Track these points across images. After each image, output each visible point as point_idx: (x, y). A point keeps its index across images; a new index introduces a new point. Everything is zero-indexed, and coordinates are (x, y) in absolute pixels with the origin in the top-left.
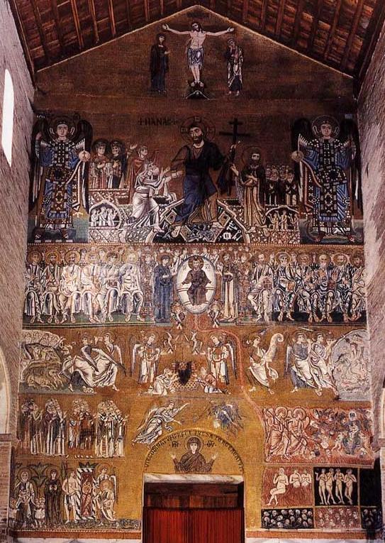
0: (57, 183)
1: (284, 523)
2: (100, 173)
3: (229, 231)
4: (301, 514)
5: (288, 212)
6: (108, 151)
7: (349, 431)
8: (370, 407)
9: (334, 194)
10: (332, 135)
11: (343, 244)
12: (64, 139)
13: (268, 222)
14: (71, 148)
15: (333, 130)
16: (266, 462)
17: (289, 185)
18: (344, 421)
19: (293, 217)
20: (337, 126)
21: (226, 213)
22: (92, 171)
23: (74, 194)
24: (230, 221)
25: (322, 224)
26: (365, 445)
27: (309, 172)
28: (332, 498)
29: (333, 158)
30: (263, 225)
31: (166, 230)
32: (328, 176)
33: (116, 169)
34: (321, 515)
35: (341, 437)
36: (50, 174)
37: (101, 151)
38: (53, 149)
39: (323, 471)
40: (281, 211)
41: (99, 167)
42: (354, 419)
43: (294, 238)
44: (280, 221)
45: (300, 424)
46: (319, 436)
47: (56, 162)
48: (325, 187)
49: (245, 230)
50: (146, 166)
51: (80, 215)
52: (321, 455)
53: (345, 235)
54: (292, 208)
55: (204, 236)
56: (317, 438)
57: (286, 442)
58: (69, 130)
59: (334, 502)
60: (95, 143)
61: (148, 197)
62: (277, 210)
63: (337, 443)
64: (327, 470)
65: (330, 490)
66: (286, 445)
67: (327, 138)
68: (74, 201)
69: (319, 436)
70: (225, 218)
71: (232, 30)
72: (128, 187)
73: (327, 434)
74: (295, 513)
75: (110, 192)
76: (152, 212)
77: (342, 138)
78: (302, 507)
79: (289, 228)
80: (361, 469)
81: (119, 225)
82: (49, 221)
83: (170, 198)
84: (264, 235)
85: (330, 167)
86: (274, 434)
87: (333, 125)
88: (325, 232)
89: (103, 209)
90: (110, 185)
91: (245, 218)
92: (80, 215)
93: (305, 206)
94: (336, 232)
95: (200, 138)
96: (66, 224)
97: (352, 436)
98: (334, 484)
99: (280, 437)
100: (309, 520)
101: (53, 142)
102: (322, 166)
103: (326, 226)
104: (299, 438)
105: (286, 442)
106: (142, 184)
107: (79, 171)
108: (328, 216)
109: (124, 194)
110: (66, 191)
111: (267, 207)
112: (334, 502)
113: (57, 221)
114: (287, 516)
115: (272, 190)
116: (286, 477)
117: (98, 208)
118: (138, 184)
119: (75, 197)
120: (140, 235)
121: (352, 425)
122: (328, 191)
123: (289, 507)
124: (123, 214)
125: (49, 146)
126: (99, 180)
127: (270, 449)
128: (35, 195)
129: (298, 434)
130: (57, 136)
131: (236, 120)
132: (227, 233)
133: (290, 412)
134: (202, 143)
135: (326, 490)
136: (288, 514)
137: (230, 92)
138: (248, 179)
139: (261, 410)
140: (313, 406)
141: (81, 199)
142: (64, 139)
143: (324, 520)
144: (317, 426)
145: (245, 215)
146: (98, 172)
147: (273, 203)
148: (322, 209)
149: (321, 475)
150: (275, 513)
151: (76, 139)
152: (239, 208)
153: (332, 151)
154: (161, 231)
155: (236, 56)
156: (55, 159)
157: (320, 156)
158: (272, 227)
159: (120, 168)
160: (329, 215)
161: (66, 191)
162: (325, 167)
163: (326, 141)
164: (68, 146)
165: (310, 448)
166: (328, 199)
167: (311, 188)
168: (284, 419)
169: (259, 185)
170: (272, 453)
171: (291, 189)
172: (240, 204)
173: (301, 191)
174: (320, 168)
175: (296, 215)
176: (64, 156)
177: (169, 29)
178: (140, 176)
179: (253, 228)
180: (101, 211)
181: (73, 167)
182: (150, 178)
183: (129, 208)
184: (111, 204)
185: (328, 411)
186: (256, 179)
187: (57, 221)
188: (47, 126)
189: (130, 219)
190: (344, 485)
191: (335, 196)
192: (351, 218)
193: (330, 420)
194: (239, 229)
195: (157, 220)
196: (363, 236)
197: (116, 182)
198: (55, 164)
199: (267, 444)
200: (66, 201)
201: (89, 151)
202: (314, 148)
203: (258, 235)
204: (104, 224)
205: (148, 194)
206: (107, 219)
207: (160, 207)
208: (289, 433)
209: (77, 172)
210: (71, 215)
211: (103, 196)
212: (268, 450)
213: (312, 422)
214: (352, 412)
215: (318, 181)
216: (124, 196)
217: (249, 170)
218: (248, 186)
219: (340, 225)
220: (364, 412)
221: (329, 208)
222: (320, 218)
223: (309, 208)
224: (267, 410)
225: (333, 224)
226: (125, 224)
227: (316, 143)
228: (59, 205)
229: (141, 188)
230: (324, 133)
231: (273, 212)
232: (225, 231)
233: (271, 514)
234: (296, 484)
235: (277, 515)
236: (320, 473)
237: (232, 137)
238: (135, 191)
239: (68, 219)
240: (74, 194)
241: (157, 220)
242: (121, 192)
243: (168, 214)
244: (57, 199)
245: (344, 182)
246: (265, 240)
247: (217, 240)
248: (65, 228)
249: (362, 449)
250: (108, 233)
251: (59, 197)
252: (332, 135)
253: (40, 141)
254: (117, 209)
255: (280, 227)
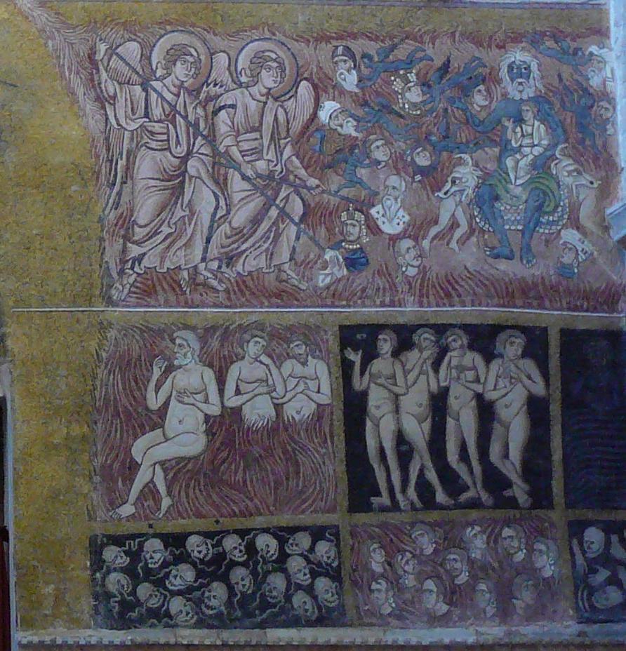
1: (199, 602)
4: (283, 557)
7: (506, 148)
8: (600, 33)
16: (110, 302)
18: (479, 100)
26: (584, 213)
28: (432, 476)
34: (377, 560)
35: (467, 174)
39: (386, 344)
42: (529, 92)
45: (269, 119)
46: (363, 173)
52: (374, 265)
56: (356, 182)
57: (205, 200)
59: (441, 497)
63: (449, 208)
64: (405, 338)
65: (418, 432)
66: (206, 219)
69: (363, 173)
73: (399, 164)
74: (251, 549)
78: (285, 519)
80: (564, 332)
86: (146, 166)
97: (519, 169)
98: (439, 404)
99: (175, 181)
100: (322, 584)
104: (268, 185)
105: (205, 200)
112: (441, 497)
114: (216, 568)
116: (209, 375)
121: (520, 120)
123: (227, 523)
127: (127, 238)
129: (261, 165)
133: (222, 59)
135: (400, 438)
136: (220, 558)
139: (83, 50)
140: (332, 27)
143: (395, 583)
144: (349, 128)
149: (377, 365)
150: (155, 552)
165: (322, 232)
168: (194, 92)
170: (139, 259)
185: (402, 53)
190: (486, 411)
193: (415, 95)
199: (112, 216)
208: (220, 167)
212: (118, 245)
213: (329, 107)
214: (518, 55)
220: (578, 59)
224: (112, 51)
233: (135, 556)
234: (258, 411)
235: (165, 564)
236: (370, 355)
249: (570, 235)
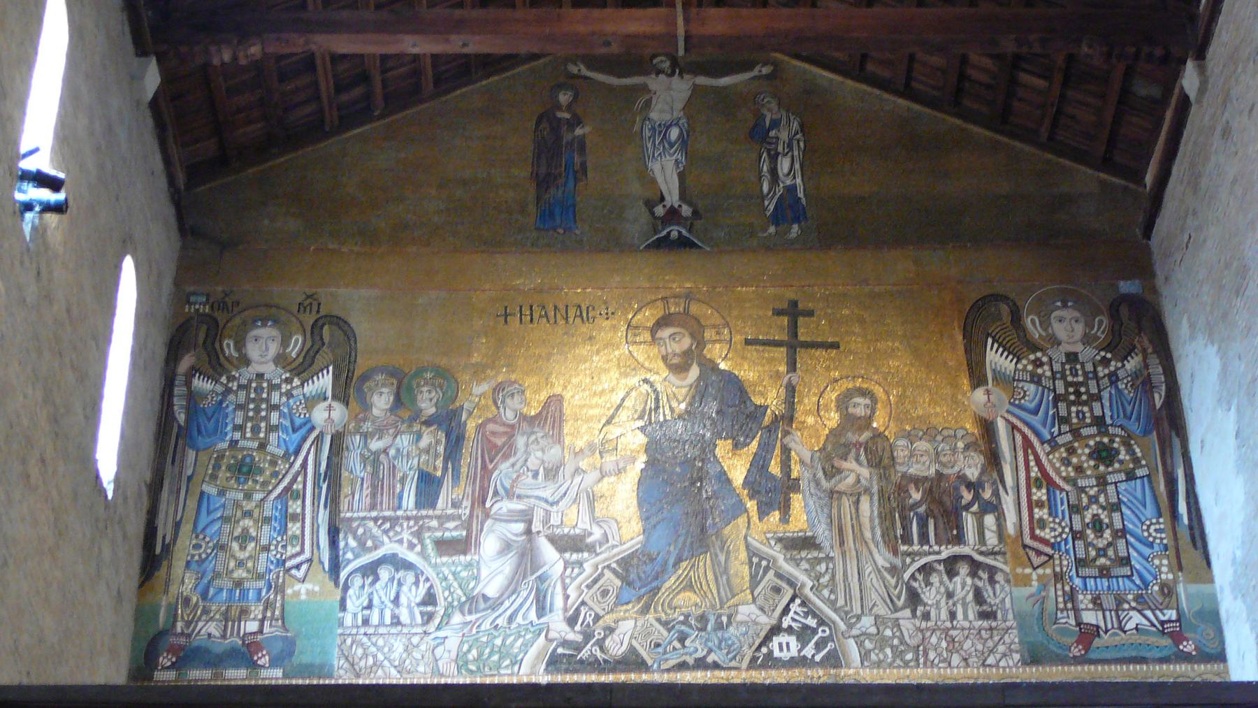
0: (240, 496)
2: (376, 463)
3: (790, 630)
5: (975, 567)
6: (401, 400)
9: (1115, 507)
10: (1087, 340)
11: (1162, 660)
12: (269, 369)
13: (914, 598)
14: (289, 395)
15: (1089, 325)
17: (969, 485)
19: (992, 581)
20: (1099, 312)
21: (779, 576)
22: (354, 464)
23: (294, 528)
24: (792, 600)
25: (1084, 600)
27: (1027, 444)
29: (1097, 406)
30: (896, 610)
31: (588, 636)
32: (1090, 456)
33: (427, 451)
36: (217, 467)
37: (381, 401)
38: (231, 397)
40: (951, 565)
41: (375, 445)
43: (1001, 648)
44: (950, 595)
47: (237, 435)
48: (1082, 490)
49: (842, 626)
50: (521, 441)
51: (308, 592)
53: (1163, 632)
54: (981, 553)
55: (710, 651)
58: (285, 343)
60: (365, 378)
61: (528, 532)
62: (939, 562)
67: (1071, 349)
68: (291, 550)
70: (777, 590)
71: (766, 70)
72: (467, 503)
75: (408, 518)
76: (541, 579)
77: (1117, 345)
79: (984, 615)
81: (437, 621)
82: (206, 611)
83: (597, 534)
84: (902, 641)
85: (1093, 430)
87: (1089, 312)
88: (1098, 627)
89: (384, 573)
90: (409, 500)
91: (841, 587)
92: (308, 592)
93: (1025, 546)
94: (1130, 626)
95: (687, 354)
96: (262, 621)
101: (234, 378)
102: (1065, 428)
103: (1097, 603)
106: (510, 494)
107: (313, 459)
108: (1102, 576)
109: (451, 525)
110: (267, 520)
111: (909, 554)
113: (234, 612)
115: (917, 504)
117: (371, 571)
118: (496, 493)
119: (295, 537)
120: (503, 652)
122: (1093, 500)
124: (449, 588)
125: (219, 389)
126: (374, 487)
128: (164, 529)
130: (245, 361)
131: (794, 304)
132: (783, 638)
134: (694, 372)
137: (772, 229)
138: (839, 471)
141: (316, 544)
142: (269, 369)
145: (839, 576)
146: (373, 461)
147: (924, 538)
148: (1081, 554)
151: (304, 368)
152: (818, 561)
153: (1092, 384)
154: (571, 636)
155: (784, 136)
156: (237, 428)
157: (1057, 399)
158: (926, 616)
159: (441, 449)
160: (1104, 573)
161: (267, 520)
162: (1075, 433)
163: (1072, 357)
164: (278, 387)
166: (1098, 526)
167: (1040, 494)
169: (875, 489)
171: (977, 497)
172: (817, 547)
173: (1008, 502)
174: (1060, 434)
175: (999, 577)
176: (267, 419)
177: (585, 72)
178: (503, 472)
179: (867, 623)
180: (377, 579)
181: (292, 449)
182: (536, 475)
183: (468, 566)
184: (412, 557)
186: (865, 472)
187: (234, 612)
188: (215, 331)
189: (473, 603)
191: (1116, 516)
192: (1175, 581)
194: (822, 622)
195: (559, 602)
196: (1220, 631)
197: (428, 486)
198: (233, 443)
200: (266, 549)
201: (346, 402)
202: (1036, 379)
203: (882, 642)
204: (388, 620)
205: (530, 522)
206: (396, 601)
207: (567, 564)
209: (304, 465)
210: (280, 590)
211: (386, 532)
215: (1058, 472)
216: (453, 531)
217: (845, 445)
218: (840, 493)
219: (1142, 602)
221: (1102, 552)
222: (1078, 581)
223: (1039, 553)
225: (1120, 601)
226: (457, 618)
227: (1041, 364)
228: (241, 564)
229: (506, 506)
230: (1060, 330)
231: (926, 570)
232: (776, 630)
237: (784, 349)
238: (487, 515)
239: (268, 605)
240: (294, 528)
241: (559, 602)
242: (443, 519)
243: (595, 581)
244: (235, 546)
245: (1139, 472)
246: (909, 656)
247: (754, 659)
248: (261, 631)
250: (398, 646)
251: (244, 538)
252: (1087, 340)
253: (193, 371)
254: (430, 572)
255: (953, 615)
